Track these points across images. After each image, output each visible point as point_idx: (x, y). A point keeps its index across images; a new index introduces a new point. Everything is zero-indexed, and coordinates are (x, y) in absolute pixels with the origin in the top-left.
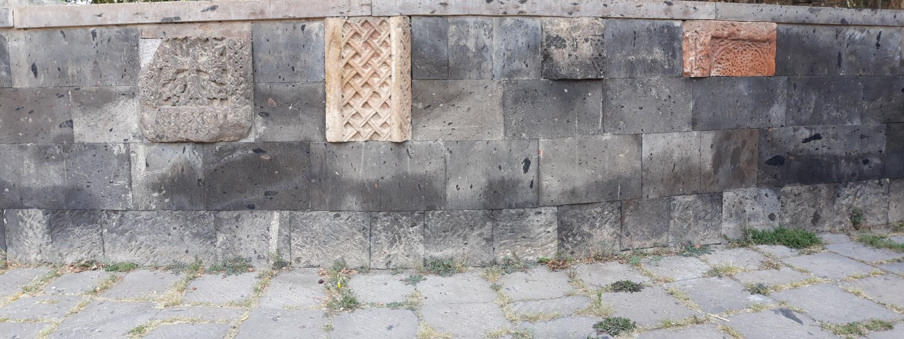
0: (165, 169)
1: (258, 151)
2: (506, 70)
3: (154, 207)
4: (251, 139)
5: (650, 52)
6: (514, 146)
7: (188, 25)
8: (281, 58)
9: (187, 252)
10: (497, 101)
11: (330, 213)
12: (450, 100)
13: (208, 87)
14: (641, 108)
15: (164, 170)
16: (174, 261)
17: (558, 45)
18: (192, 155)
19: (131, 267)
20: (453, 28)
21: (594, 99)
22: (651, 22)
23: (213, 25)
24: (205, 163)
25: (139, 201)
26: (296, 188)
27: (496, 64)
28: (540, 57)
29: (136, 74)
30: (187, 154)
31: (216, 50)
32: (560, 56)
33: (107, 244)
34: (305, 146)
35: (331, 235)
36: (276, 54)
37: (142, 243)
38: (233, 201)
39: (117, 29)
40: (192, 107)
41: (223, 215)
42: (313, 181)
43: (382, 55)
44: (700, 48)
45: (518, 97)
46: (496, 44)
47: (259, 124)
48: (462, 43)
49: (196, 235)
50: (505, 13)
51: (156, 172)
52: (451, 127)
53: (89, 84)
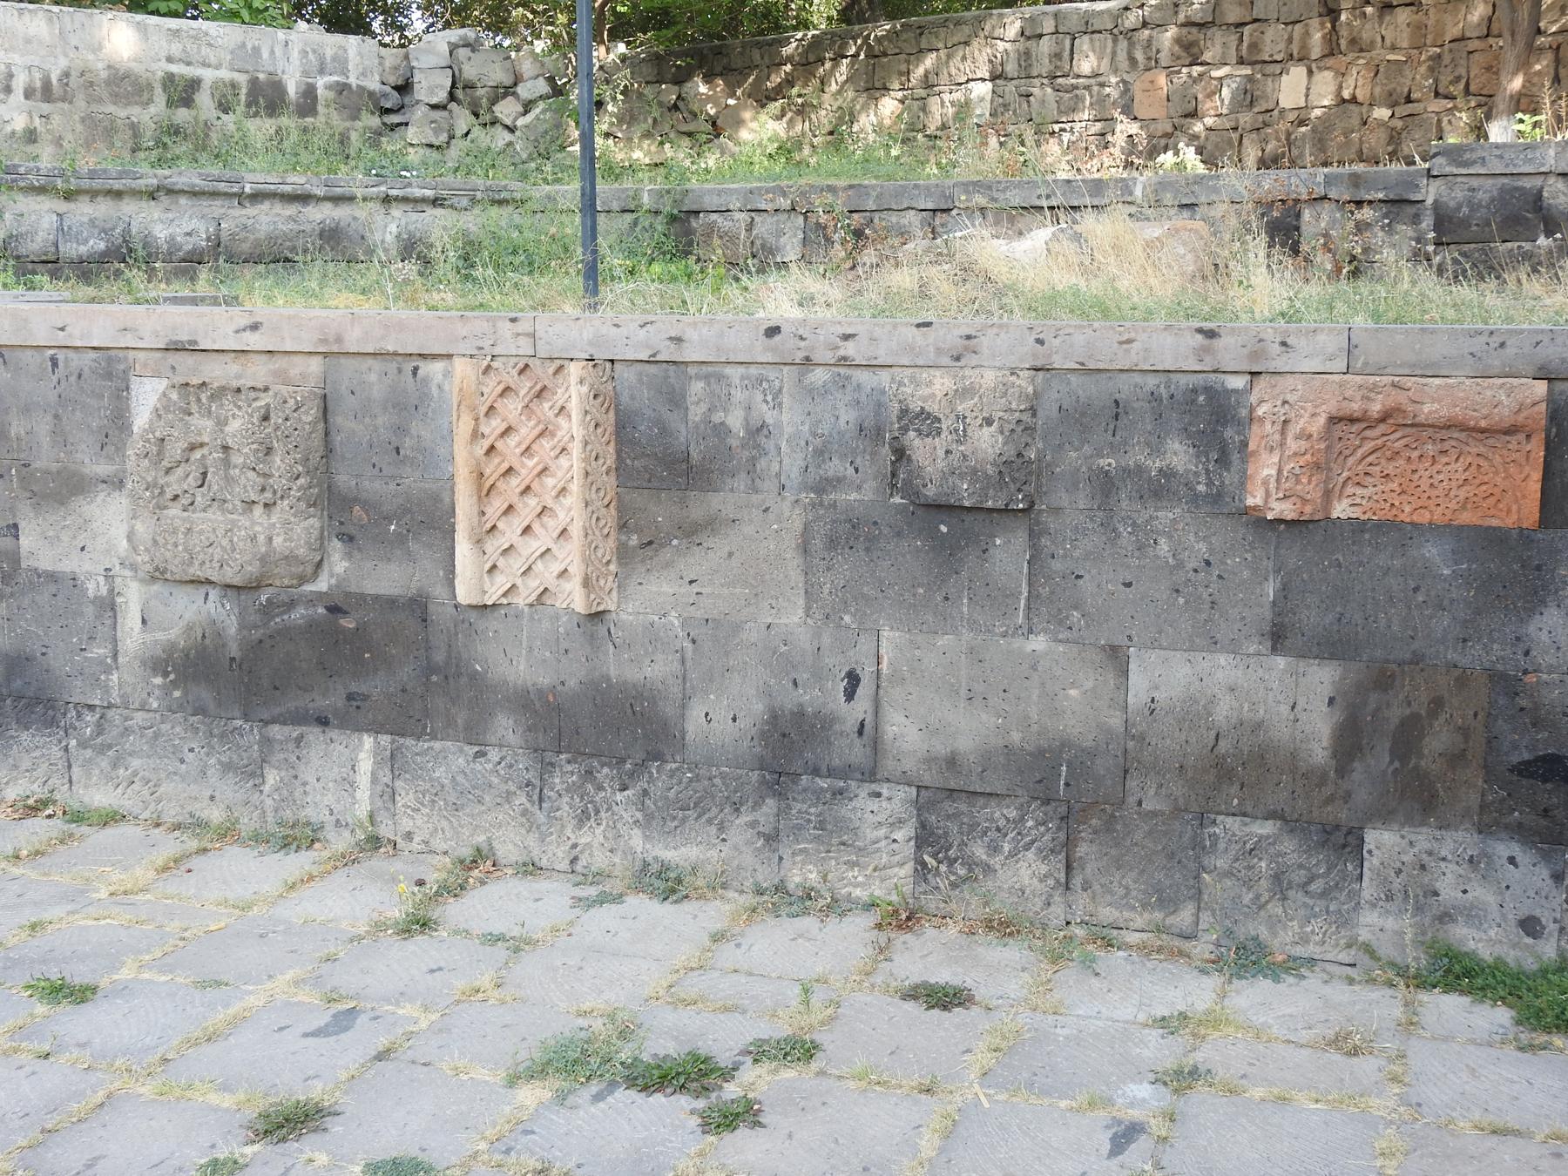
0: (174, 634)
1: (334, 610)
2: (813, 475)
3: (155, 705)
4: (322, 585)
5: (1156, 450)
6: (826, 640)
8: (376, 429)
9: (212, 798)
10: (790, 541)
11: (467, 748)
12: (693, 532)
13: (243, 481)
14: (1129, 585)
16: (191, 815)
17: (924, 428)
18: (220, 609)
19: (111, 818)
20: (697, 387)
21: (1007, 553)
22: (1162, 378)
24: (242, 626)
25: (129, 690)
26: (404, 691)
27: (788, 461)
28: (886, 450)
30: (211, 605)
32: (928, 454)
33: (76, 770)
34: (418, 606)
35: (463, 793)
36: (367, 420)
37: (135, 774)
38: (292, 705)
39: (93, 355)
40: (214, 515)
41: (276, 731)
42: (434, 678)
43: (559, 434)
44: (1293, 445)
45: (839, 536)
46: (789, 420)
48: (718, 417)
49: (227, 767)
50: (807, 359)
51: (161, 636)
52: (695, 588)
53: (45, 458)
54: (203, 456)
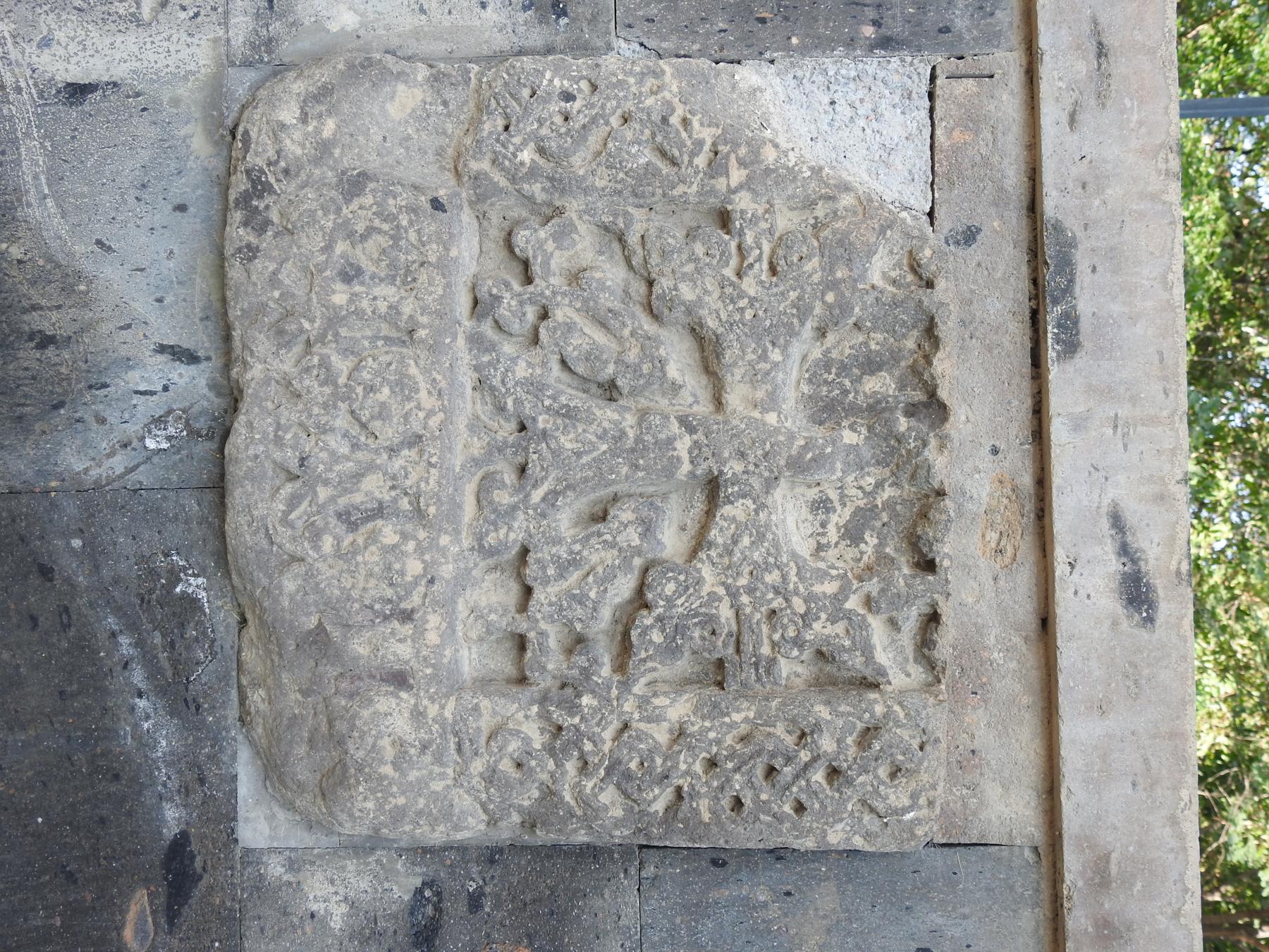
1: (179, 871)
4: (259, 825)
7: (1021, 405)
13: (598, 556)
15: (41, 211)
23: (1025, 578)
29: (688, 30)
30: (153, 372)
31: (857, 626)
47: (359, 879)
54: (676, 388)
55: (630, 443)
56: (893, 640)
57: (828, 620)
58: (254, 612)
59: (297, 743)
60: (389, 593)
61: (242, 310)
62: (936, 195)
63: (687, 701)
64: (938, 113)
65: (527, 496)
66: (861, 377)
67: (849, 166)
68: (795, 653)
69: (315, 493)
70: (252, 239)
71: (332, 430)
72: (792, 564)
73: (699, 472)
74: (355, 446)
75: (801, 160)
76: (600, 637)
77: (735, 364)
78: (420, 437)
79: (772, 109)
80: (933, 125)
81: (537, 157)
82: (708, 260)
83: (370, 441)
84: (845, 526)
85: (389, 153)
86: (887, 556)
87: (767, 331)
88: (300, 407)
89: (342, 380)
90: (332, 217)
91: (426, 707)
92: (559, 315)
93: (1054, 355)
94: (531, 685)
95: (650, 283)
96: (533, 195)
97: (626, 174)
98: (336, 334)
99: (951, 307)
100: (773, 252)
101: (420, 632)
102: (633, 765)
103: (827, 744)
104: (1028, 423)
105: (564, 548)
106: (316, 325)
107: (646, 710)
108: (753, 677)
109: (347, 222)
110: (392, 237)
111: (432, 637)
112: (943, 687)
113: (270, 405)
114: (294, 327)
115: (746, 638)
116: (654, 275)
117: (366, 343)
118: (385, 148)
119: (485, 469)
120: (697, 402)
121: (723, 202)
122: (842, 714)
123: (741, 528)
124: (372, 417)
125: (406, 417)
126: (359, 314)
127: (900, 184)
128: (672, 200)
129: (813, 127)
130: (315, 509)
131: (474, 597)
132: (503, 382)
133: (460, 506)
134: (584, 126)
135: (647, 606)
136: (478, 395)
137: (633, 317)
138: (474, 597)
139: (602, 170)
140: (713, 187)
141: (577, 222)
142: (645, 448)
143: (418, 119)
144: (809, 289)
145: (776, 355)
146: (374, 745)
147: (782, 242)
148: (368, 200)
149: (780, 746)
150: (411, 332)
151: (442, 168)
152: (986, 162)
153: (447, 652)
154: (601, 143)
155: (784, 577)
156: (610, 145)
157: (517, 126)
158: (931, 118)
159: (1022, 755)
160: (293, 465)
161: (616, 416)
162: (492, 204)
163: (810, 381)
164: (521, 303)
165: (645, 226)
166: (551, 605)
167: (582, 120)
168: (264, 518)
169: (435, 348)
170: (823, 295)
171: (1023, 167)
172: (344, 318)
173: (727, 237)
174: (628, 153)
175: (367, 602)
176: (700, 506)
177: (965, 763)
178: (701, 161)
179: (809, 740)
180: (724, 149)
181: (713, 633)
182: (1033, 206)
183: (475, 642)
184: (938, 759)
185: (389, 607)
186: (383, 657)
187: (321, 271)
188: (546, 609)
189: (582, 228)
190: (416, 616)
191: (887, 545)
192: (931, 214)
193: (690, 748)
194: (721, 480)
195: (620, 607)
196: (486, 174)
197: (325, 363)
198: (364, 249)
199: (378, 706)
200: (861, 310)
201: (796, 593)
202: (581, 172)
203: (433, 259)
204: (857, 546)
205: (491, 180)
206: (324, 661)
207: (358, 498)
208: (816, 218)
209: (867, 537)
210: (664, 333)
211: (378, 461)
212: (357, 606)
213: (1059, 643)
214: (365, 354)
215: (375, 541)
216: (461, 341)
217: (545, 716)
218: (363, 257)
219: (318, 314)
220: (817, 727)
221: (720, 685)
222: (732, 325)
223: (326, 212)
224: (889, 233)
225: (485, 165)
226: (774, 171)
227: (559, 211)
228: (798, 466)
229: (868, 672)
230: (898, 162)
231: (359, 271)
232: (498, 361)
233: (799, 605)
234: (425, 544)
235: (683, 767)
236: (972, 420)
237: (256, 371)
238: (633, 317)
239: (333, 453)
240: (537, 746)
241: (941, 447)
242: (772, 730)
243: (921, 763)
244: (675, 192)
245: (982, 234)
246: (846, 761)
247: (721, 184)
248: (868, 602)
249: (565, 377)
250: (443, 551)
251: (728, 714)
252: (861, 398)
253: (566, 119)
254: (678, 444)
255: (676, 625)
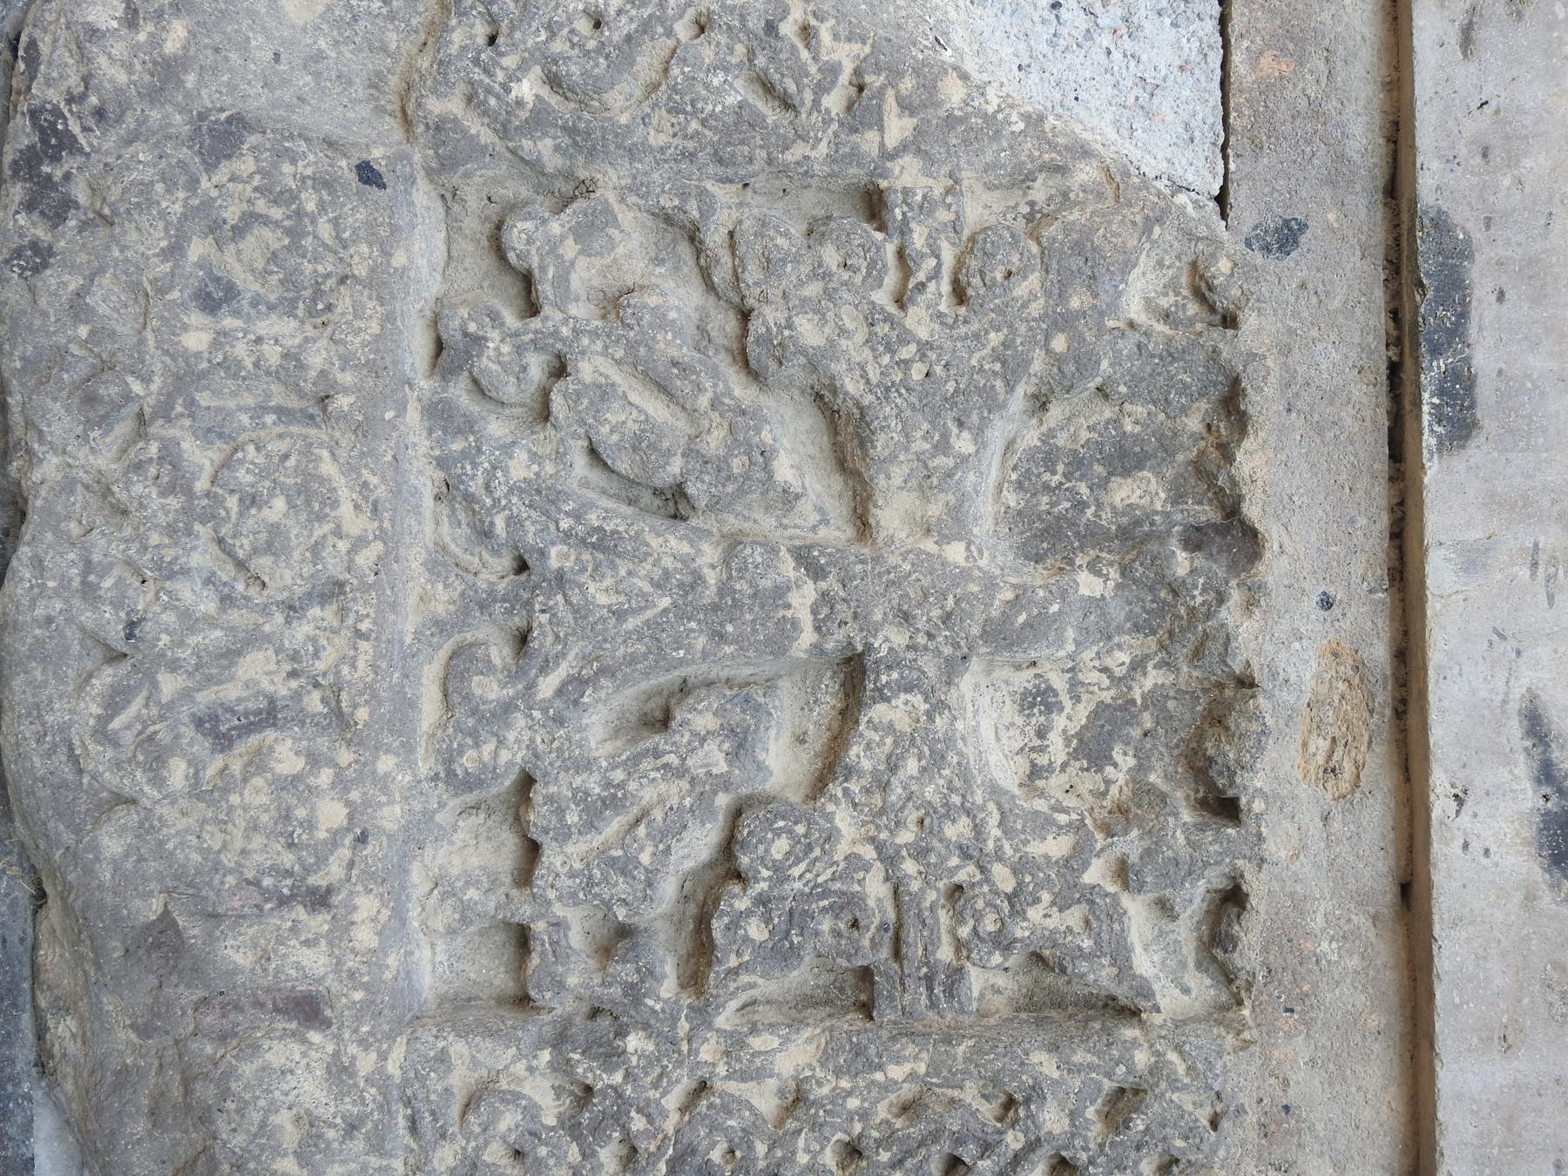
7: (1372, 527)
13: (651, 790)
23: (1374, 817)
40: (422, 580)
54: (789, 499)
55: (709, 594)
56: (1161, 933)
57: (1053, 903)
58: (54, 885)
59: (130, 1116)
60: (288, 859)
61: (22, 359)
62: (1232, 167)
63: (809, 1040)
64: (1236, 26)
65: (531, 686)
66: (1107, 480)
67: (1083, 115)
68: (997, 958)
69: (155, 685)
70: (41, 233)
71: (185, 572)
72: (991, 806)
73: (830, 645)
74: (227, 601)
75: (1008, 103)
76: (659, 924)
77: (893, 458)
78: (341, 585)
79: (952, 15)
80: (1226, 46)
81: (545, 92)
82: (846, 276)
83: (253, 591)
84: (1079, 735)
85: (285, 82)
86: (1152, 790)
87: (950, 400)
88: (128, 532)
89: (201, 485)
90: (181, 195)
91: (354, 1058)
92: (586, 370)
93: (1433, 441)
94: (538, 1010)
95: (745, 315)
96: (539, 160)
97: (703, 122)
98: (191, 403)
99: (1269, 362)
100: (960, 263)
101: (342, 928)
102: (716, 1155)
103: (1052, 1120)
104: (1382, 555)
105: (596, 777)
106: (154, 387)
107: (739, 1060)
108: (924, 1000)
109: (208, 203)
110: (288, 232)
111: (364, 937)
112: (1246, 1012)
113: (74, 528)
114: (114, 390)
115: (911, 934)
116: (750, 302)
117: (245, 419)
118: (276, 73)
119: (457, 637)
120: (825, 521)
121: (872, 174)
122: (1075, 1069)
123: (904, 743)
124: (255, 551)
125: (316, 550)
126: (231, 367)
127: (1171, 148)
128: (783, 170)
129: (1022, 47)
130: (154, 711)
131: (439, 861)
132: (487, 487)
133: (413, 704)
134: (628, 38)
135: (738, 876)
136: (444, 509)
137: (715, 374)
138: (439, 861)
139: (661, 116)
140: (855, 147)
141: (616, 207)
142: (736, 604)
143: (338, 23)
144: (1023, 329)
145: (963, 443)
146: (263, 1125)
147: (975, 244)
148: (246, 165)
149: (973, 1125)
150: (324, 400)
151: (380, 110)
152: (1316, 110)
153: (392, 960)
154: (660, 68)
155: (978, 829)
156: (675, 71)
157: (510, 35)
158: (1223, 33)
159: (1368, 1114)
160: (115, 634)
161: (685, 548)
162: (467, 175)
163: (1020, 486)
164: (519, 350)
165: (735, 214)
166: (572, 875)
167: (625, 26)
168: (63, 728)
169: (366, 429)
170: (1048, 338)
171: (1378, 120)
172: (203, 375)
173: (879, 236)
174: (707, 86)
175: (250, 875)
176: (829, 700)
177: (1273, 1127)
178: (834, 102)
179: (1022, 1113)
180: (874, 80)
181: (855, 924)
182: (1395, 187)
183: (441, 935)
184: (1243, 1143)
185: (289, 882)
186: (277, 971)
187: (161, 291)
188: (564, 882)
189: (625, 217)
190: (336, 900)
191: (1151, 769)
192: (1221, 199)
193: (816, 1126)
194: (869, 661)
195: (694, 874)
196: (455, 120)
197: (170, 455)
198: (239, 252)
199: (268, 1056)
200: (1112, 365)
201: (999, 856)
202: (624, 119)
203: (361, 271)
204: (1100, 770)
205: (465, 132)
206: (174, 979)
207: (231, 692)
208: (1032, 204)
209: (1117, 754)
210: (767, 402)
211: (267, 628)
212: (231, 880)
213: (1437, 931)
214: (244, 437)
215: (262, 769)
216: (413, 415)
217: (562, 1066)
218: (237, 265)
219: (157, 367)
220: (1035, 1093)
221: (867, 1009)
222: (888, 389)
223: (171, 187)
224: (1157, 230)
225: (453, 105)
226: (960, 120)
227: (585, 188)
228: (1002, 637)
229: (1122, 992)
230: (1166, 109)
231: (231, 291)
232: (479, 449)
233: (1003, 878)
234: (351, 774)
235: (803, 1159)
236: (1289, 549)
237: (49, 469)
238: (715, 374)
239: (186, 615)
240: (550, 1121)
241: (1250, 605)
242: (956, 1093)
243: (1214, 1152)
244: (791, 156)
245: (1308, 234)
246: (1085, 1149)
247: (869, 142)
248: (1123, 872)
249: (597, 477)
250: (384, 783)
251: (880, 1067)
252: (1106, 515)
253: (597, 25)
254: (794, 598)
255: (791, 913)
